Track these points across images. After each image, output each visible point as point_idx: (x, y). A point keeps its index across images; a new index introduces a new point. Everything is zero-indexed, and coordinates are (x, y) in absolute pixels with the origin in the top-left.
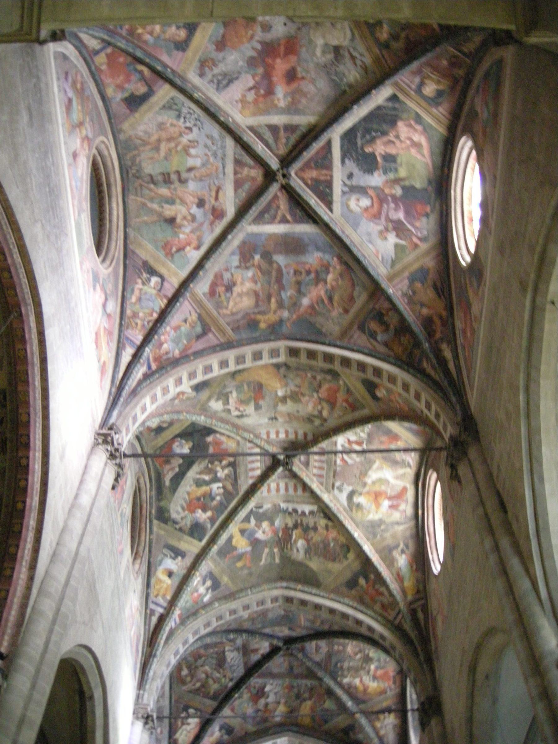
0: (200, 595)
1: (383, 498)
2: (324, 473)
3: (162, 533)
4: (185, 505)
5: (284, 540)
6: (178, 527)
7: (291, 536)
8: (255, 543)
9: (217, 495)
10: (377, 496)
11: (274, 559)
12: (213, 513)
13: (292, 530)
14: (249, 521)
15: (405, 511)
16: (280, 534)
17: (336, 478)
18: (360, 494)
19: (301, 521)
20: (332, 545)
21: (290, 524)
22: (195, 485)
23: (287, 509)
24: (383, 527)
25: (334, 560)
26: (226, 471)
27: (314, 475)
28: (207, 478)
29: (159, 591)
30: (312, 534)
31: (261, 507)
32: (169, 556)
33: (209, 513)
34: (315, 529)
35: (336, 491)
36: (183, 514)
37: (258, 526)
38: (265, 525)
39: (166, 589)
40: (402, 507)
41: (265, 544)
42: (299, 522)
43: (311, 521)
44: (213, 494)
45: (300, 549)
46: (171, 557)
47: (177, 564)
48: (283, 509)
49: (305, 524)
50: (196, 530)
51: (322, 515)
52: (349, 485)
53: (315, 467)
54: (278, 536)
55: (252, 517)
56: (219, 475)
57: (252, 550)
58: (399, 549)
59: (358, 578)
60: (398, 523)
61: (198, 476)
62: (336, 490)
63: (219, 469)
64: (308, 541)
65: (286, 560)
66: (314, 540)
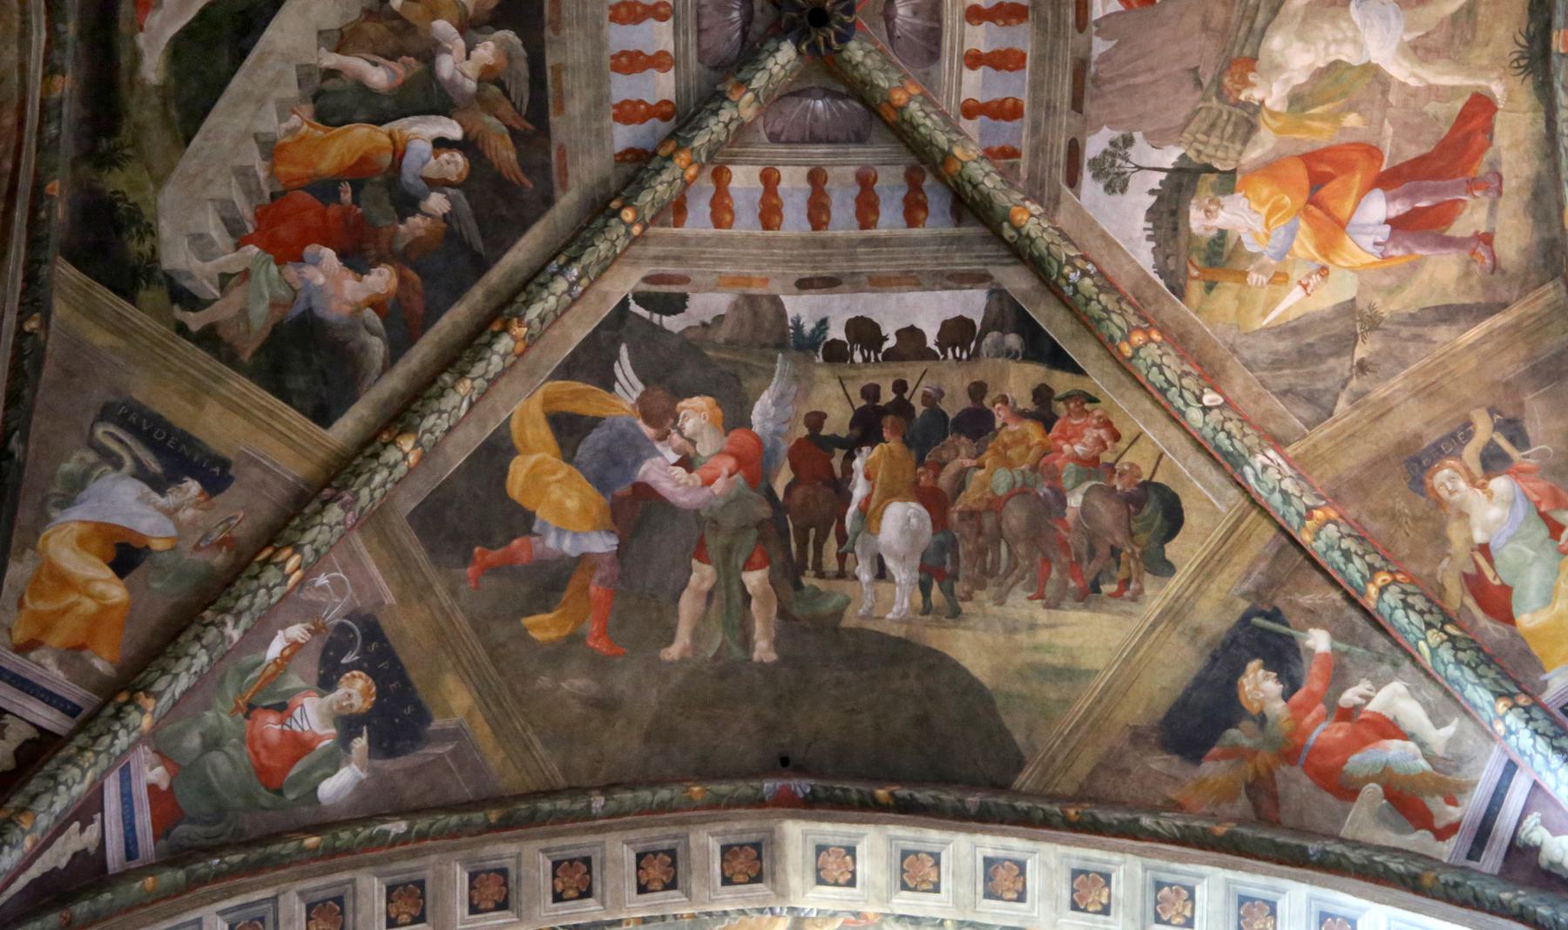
0: (300, 745)
1: (1357, 180)
2: (1015, 87)
3: (101, 338)
4: (245, 210)
5: (799, 514)
6: (195, 321)
7: (840, 490)
8: (636, 511)
9: (436, 184)
10: (1320, 176)
11: (747, 643)
12: (402, 280)
13: (850, 457)
14: (607, 381)
15: (1487, 239)
16: (781, 481)
17: (1087, 104)
18: (1228, 182)
19: (900, 387)
20: (1075, 501)
21: (838, 420)
22: (308, 110)
23: (823, 324)
24: (1360, 352)
25: (1089, 594)
26: (486, 51)
27: (970, 110)
28: (378, 76)
29: (46, 624)
30: (959, 455)
31: (675, 304)
32: (129, 463)
33: (382, 279)
34: (977, 423)
35: (1090, 188)
36: (231, 260)
37: (661, 417)
38: (696, 414)
39: (95, 622)
40: (1472, 218)
41: (697, 534)
42: (888, 396)
43: (951, 383)
44: (409, 174)
45: (890, 563)
46: (141, 473)
47: (171, 513)
48: (798, 326)
49: (920, 410)
50: (303, 359)
51: (1013, 341)
52: (1158, 139)
53: (974, 60)
54: (770, 494)
55: (624, 351)
56: (446, 66)
57: (621, 553)
58: (1471, 452)
59: (1239, 670)
60: (1449, 314)
61: (331, 60)
62: (1087, 175)
63: (443, 27)
64: (936, 502)
65: (815, 633)
66: (970, 497)
